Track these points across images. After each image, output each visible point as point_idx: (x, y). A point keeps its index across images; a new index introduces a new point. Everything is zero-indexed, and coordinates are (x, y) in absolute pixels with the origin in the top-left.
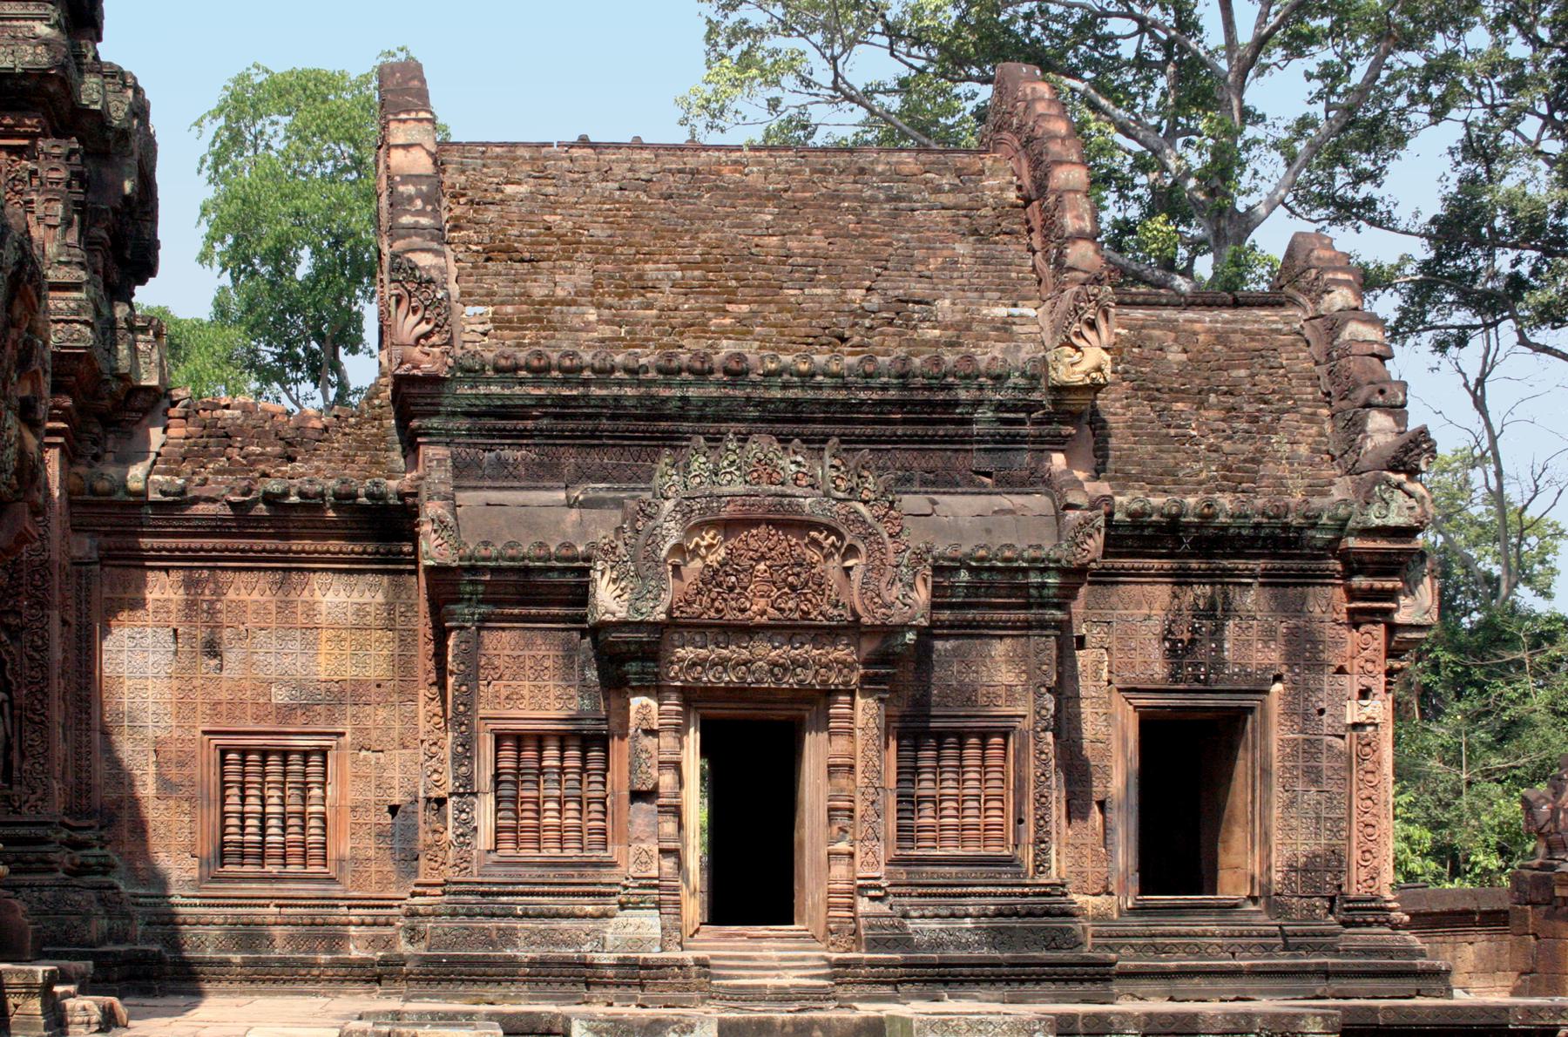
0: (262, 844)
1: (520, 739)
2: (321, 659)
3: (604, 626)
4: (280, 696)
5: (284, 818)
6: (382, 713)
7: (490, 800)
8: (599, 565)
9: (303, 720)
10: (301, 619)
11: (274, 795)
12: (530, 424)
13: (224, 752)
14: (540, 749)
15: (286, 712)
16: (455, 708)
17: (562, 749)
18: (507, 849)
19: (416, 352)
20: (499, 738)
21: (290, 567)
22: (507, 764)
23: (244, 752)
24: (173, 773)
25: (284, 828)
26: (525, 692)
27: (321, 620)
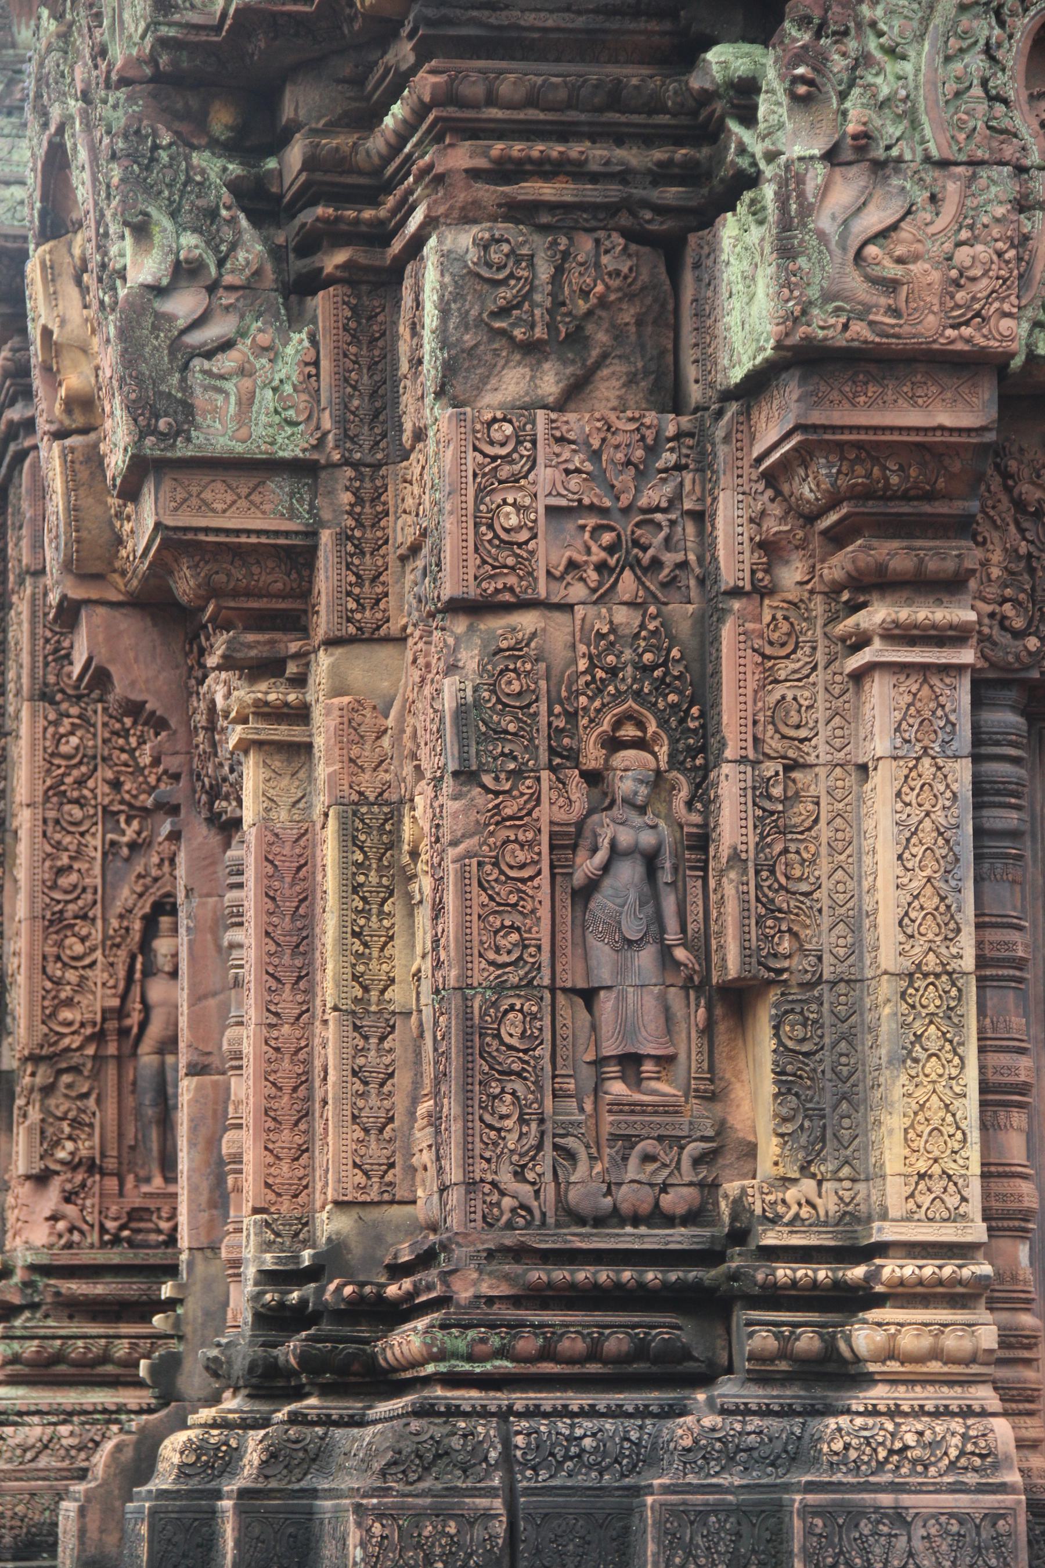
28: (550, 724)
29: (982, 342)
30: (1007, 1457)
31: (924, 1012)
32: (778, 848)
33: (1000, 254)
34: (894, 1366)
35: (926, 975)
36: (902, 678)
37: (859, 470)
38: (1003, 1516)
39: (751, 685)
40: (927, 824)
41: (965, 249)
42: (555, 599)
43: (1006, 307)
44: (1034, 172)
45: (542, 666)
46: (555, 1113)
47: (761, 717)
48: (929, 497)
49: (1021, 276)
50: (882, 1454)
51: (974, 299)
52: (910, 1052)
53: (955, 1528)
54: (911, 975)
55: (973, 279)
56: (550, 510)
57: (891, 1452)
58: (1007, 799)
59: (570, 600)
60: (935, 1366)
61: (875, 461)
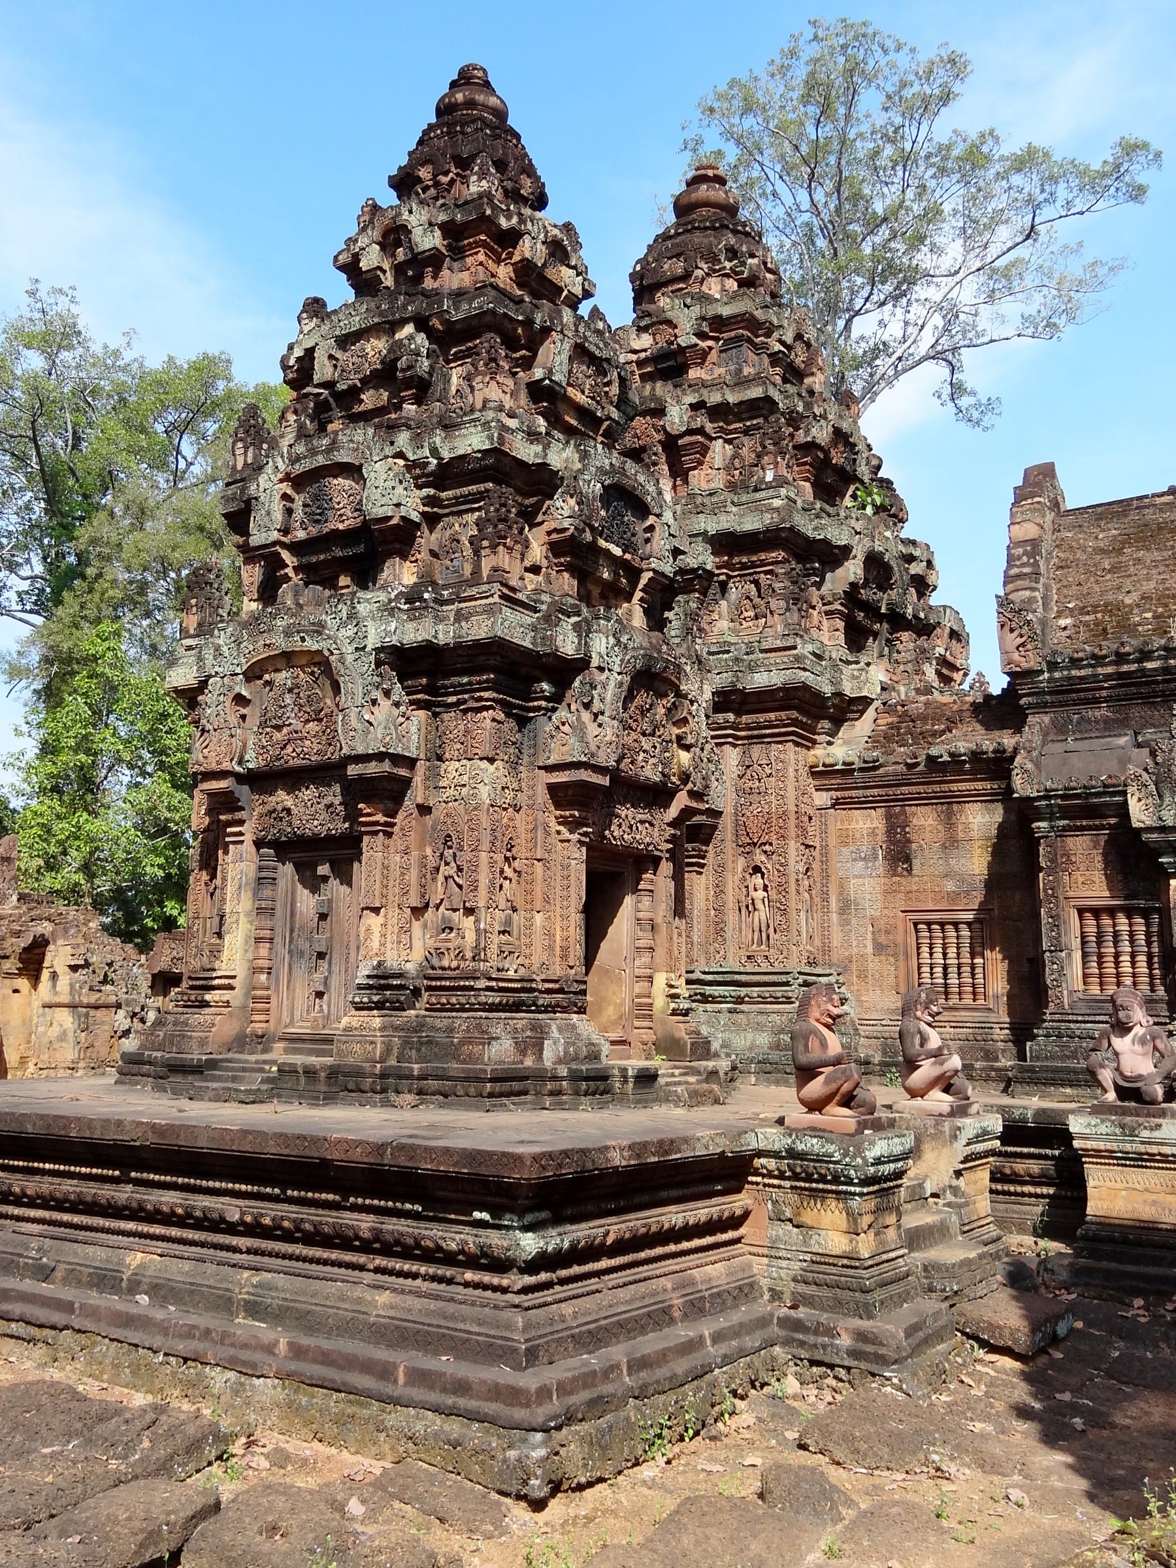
0: (946, 985)
1: (1096, 912)
2: (975, 860)
3: (1139, 831)
4: (950, 886)
5: (959, 966)
6: (1018, 896)
7: (1077, 955)
8: (1130, 790)
9: (965, 901)
10: (961, 835)
11: (952, 951)
12: (1104, 693)
13: (915, 924)
14: (1113, 917)
15: (954, 897)
16: (1045, 890)
17: (1129, 917)
18: (1095, 990)
19: (1016, 656)
20: (1081, 911)
21: (949, 803)
22: (1091, 929)
23: (929, 924)
24: (882, 939)
25: (959, 974)
26: (1097, 880)
27: (975, 834)
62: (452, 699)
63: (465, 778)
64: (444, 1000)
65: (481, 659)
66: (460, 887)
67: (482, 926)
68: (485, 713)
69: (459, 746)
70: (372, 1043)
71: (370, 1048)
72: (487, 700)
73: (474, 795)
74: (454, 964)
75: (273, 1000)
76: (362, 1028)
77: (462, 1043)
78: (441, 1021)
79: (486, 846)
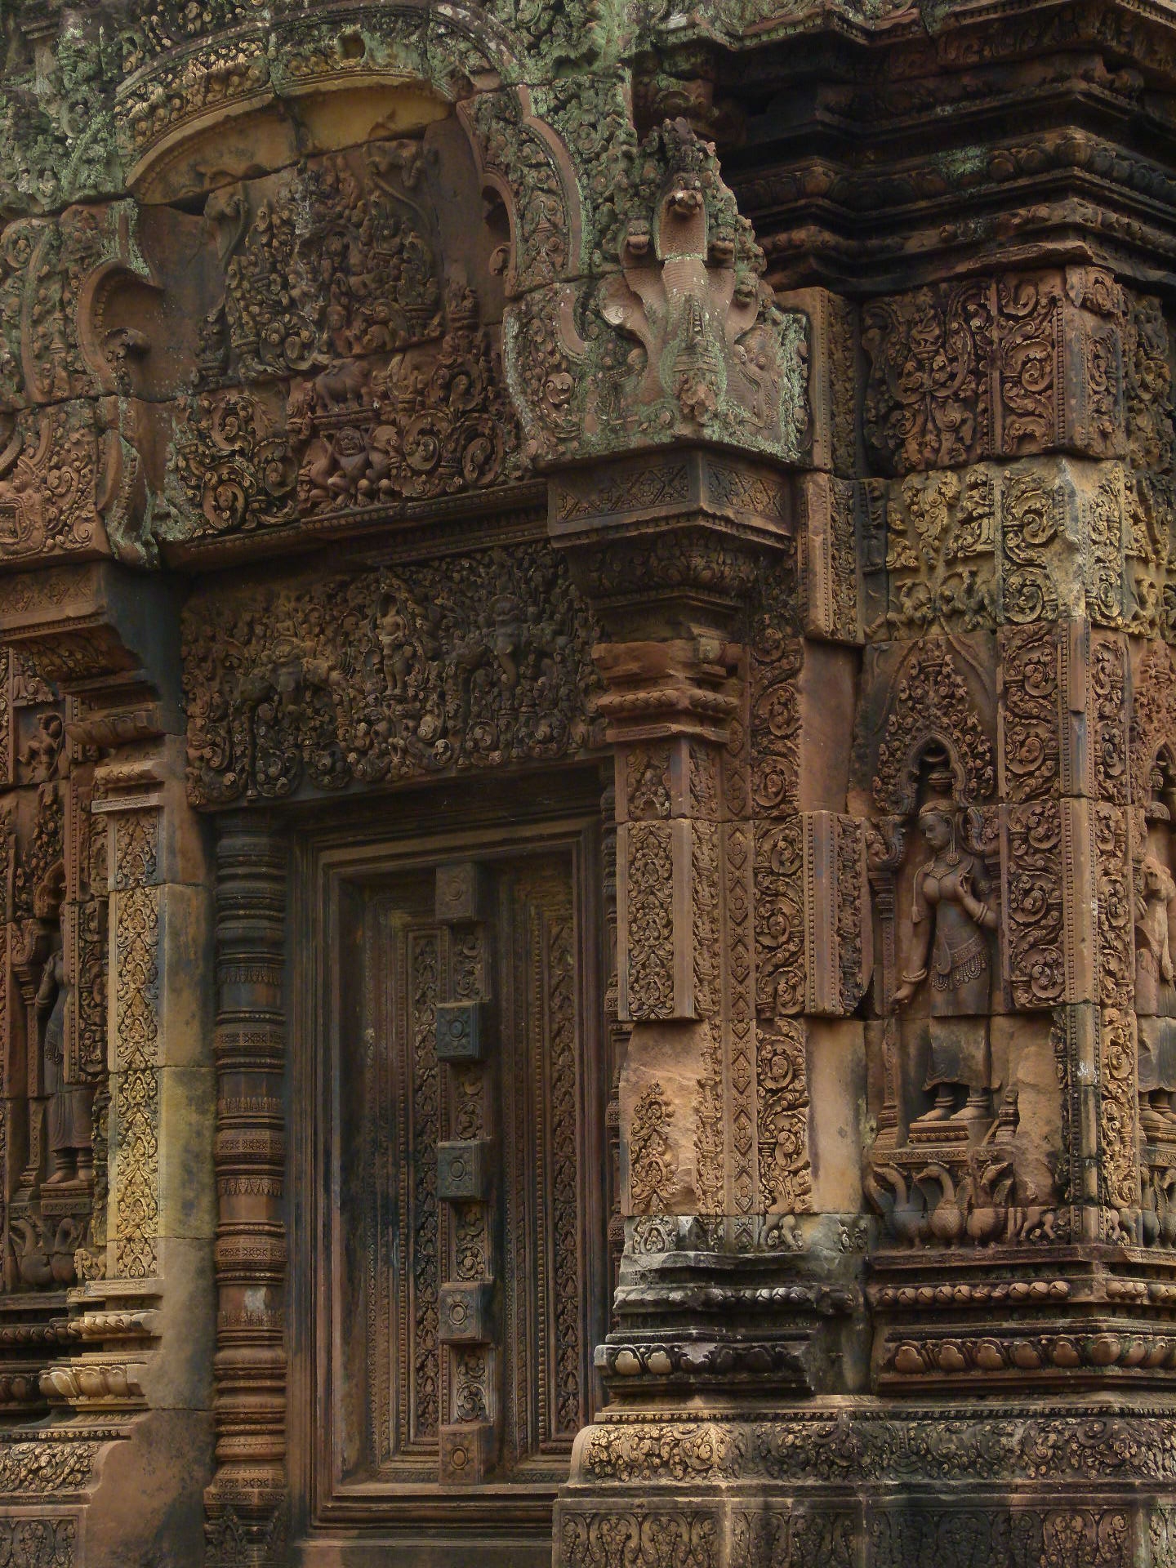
28: (14, 883)
29: (69, 545)
30: (98, 1474)
31: (133, 1102)
32: (95, 970)
33: (78, 471)
34: (83, 1400)
35: (135, 1072)
36: (123, 823)
37: (46, 661)
38: (71, 1522)
39: (79, 839)
40: (138, 944)
41: (56, 472)
42: (25, 781)
43: (84, 514)
44: (102, 399)
45: (12, 838)
46: (12, 1200)
47: (85, 865)
48: (106, 672)
49: (97, 485)
50: (24, 1473)
51: (61, 512)
52: (125, 1136)
53: (40, 1531)
54: (126, 1072)
55: (62, 496)
56: (15, 709)
57: (30, 1471)
58: (235, 912)
59: (37, 780)
60: (108, 1399)
61: (53, 651)
62: (923, 240)
63: (989, 529)
64: (952, 1352)
65: (1033, 79)
66: (988, 934)
67: (1086, 1071)
68: (1052, 285)
69: (955, 414)
70: (700, 1515)
71: (692, 1535)
72: (1062, 230)
73: (1033, 594)
74: (983, 1217)
75: (297, 1382)
76: (654, 1462)
77: (1040, 1513)
78: (950, 1431)
79: (1086, 778)
